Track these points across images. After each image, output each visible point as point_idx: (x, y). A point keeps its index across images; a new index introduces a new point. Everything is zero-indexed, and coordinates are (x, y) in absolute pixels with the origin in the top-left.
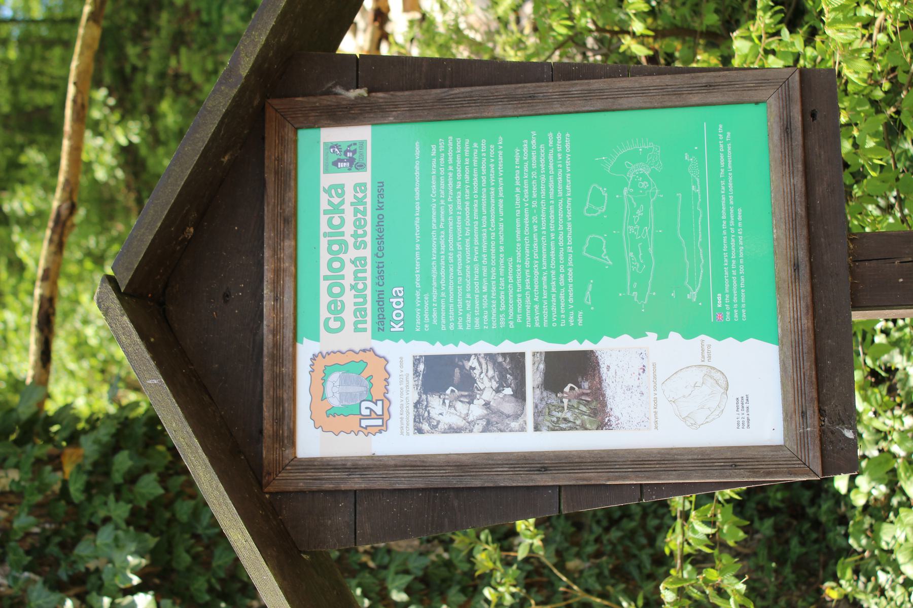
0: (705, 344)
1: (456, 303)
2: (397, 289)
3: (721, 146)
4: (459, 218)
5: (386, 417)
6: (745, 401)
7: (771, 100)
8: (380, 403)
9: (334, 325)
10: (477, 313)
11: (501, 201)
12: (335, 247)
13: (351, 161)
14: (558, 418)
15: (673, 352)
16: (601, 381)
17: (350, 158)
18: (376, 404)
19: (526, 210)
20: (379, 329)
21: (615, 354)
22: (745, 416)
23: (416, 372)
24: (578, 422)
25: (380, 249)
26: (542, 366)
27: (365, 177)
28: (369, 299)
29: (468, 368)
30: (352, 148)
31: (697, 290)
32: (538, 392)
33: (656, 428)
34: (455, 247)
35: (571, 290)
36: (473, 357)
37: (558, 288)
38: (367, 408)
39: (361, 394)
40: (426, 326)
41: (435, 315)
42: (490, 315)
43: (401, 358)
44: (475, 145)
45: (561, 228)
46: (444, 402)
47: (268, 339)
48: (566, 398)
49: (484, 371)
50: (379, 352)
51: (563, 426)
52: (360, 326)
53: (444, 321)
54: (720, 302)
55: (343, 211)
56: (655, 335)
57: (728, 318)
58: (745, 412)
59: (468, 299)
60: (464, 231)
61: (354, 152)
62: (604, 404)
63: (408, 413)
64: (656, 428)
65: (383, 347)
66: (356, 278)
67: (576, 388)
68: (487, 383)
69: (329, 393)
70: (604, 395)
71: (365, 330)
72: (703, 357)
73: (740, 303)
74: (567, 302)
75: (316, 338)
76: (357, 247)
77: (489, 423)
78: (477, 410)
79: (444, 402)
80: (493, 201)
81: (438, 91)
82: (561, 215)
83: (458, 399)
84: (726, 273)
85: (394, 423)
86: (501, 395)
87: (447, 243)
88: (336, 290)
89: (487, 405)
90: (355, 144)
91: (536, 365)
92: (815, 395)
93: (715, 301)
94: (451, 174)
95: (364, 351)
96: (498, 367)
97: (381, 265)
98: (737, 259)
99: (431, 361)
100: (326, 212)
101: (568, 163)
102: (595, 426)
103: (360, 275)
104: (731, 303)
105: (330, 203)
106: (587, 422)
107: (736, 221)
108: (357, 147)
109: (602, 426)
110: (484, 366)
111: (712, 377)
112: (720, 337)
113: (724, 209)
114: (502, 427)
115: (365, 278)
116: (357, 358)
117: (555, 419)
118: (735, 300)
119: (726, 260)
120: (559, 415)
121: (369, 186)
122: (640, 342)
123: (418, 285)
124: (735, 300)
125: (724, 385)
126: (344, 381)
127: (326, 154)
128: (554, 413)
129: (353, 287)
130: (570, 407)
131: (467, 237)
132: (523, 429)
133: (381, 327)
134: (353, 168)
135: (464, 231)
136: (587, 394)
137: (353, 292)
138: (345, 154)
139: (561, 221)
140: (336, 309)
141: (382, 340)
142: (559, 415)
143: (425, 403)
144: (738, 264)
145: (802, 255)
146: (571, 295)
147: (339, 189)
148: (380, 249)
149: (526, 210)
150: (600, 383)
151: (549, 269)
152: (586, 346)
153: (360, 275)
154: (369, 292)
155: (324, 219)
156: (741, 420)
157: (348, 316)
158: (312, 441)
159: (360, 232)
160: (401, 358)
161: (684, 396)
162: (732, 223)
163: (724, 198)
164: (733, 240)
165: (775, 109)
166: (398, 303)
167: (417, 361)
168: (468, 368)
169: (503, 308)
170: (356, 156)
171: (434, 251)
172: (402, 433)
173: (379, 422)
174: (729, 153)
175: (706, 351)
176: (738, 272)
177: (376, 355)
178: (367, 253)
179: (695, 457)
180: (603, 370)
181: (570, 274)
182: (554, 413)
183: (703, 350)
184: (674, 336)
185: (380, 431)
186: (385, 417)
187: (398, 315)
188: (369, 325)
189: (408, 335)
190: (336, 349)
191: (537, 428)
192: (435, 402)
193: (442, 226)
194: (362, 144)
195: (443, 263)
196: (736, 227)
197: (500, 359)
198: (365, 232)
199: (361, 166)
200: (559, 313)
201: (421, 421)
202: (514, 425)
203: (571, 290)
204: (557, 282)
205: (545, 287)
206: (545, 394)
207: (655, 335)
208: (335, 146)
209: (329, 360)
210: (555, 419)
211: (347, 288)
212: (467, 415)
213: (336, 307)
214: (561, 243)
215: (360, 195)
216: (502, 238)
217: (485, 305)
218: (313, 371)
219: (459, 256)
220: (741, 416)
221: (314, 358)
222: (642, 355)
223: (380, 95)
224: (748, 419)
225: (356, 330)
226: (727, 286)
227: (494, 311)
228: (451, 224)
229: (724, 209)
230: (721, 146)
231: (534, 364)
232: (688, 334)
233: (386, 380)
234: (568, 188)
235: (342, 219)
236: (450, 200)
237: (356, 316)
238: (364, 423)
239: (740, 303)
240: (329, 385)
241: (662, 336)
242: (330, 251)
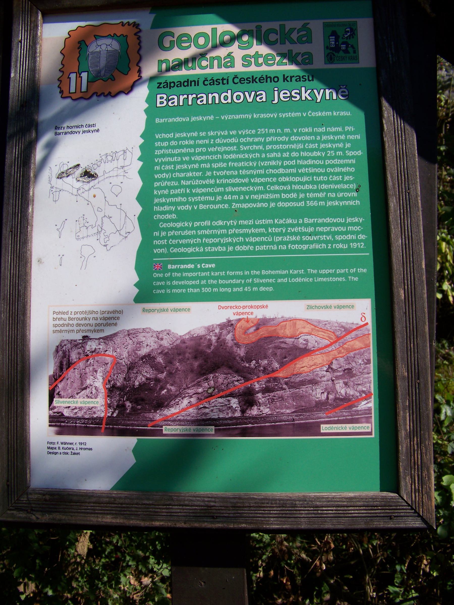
13: (337, 49)
25: (242, 81)
30: (350, 50)
55: (283, 43)
58: (62, 451)
61: (346, 51)
75: (155, 26)
76: (244, 58)
90: (355, 52)
97: (225, 82)
100: (282, 27)
103: (216, 62)
105: (292, 30)
108: (352, 54)
115: (212, 67)
134: (329, 51)
138: (343, 43)
148: (242, 81)
153: (216, 62)
155: (275, 25)
159: (261, 60)
170: (341, 54)
178: (239, 68)
190: (143, 44)
194: (355, 59)
199: (331, 59)
208: (353, 32)
213: (185, 42)
224: (56, 453)
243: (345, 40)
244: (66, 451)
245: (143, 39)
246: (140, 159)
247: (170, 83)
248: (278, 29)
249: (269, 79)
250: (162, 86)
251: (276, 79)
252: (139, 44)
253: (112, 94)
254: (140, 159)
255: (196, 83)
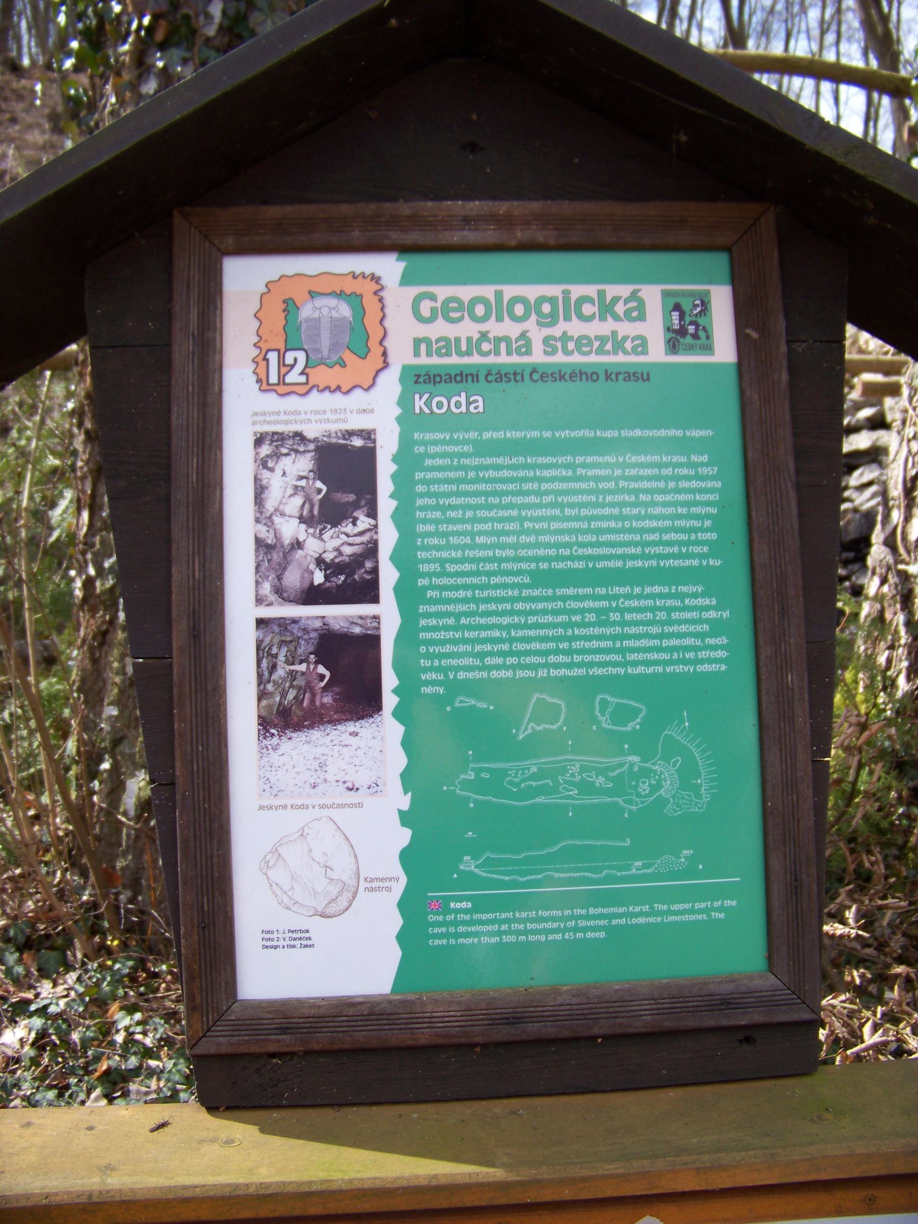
0: (393, 884)
1: (459, 494)
2: (480, 403)
3: (703, 905)
4: (594, 499)
5: (282, 389)
6: (304, 942)
7: (772, 980)
8: (303, 379)
9: (426, 307)
10: (443, 528)
11: (619, 564)
12: (546, 308)
13: (682, 332)
14: (276, 656)
15: (381, 835)
16: (333, 722)
17: (686, 330)
18: (302, 373)
19: (605, 603)
20: (419, 376)
21: (375, 747)
22: (281, 943)
23: (350, 434)
24: (270, 687)
26: (357, 630)
27: (657, 353)
28: (466, 360)
29: (355, 514)
30: (702, 334)
31: (477, 871)
32: (318, 624)
33: (262, 808)
34: (547, 492)
35: (478, 675)
36: (373, 522)
37: (482, 655)
38: (295, 360)
39: (318, 351)
40: (422, 449)
41: (439, 462)
42: (438, 548)
43: (372, 411)
44: (708, 523)
45: (577, 658)
46: (301, 478)
47: (405, 209)
48: (308, 668)
49: (350, 540)
50: (383, 377)
51: (264, 663)
52: (423, 347)
53: (429, 476)
54: (459, 905)
55: (603, 319)
56: (405, 807)
57: (432, 918)
58: (287, 942)
59: (464, 514)
60: (571, 506)
61: (695, 336)
62: (298, 727)
63: (287, 423)
64: (262, 808)
65: (390, 384)
66: (498, 340)
67: (323, 684)
68: (332, 544)
69: (319, 302)
70: (311, 727)
71: (417, 354)
72: (372, 880)
73: (458, 935)
74: (457, 669)
75: (406, 280)
76: (546, 341)
77: (269, 548)
78: (290, 529)
79: (301, 478)
80: (620, 551)
81: (791, 466)
82: (597, 658)
83: (308, 499)
84: (504, 916)
85: (271, 401)
86: (312, 567)
87: (552, 479)
88: (480, 310)
89: (298, 545)
90: (708, 337)
91: (360, 621)
92: (315, 1047)
93: (460, 899)
94: (662, 485)
95: (385, 354)
96: (357, 561)
97: (519, 377)
98: (526, 932)
99: (367, 457)
100: (601, 294)
101: (679, 669)
102: (264, 714)
103: (503, 346)
104: (456, 923)
105: (615, 300)
106: (271, 701)
107: (585, 930)
108: (704, 340)
109: (265, 724)
110: (358, 540)
111: (340, 893)
112: (403, 905)
113: (605, 911)
114: (262, 569)
115: (497, 353)
116: (373, 343)
117: (275, 650)
118: (461, 929)
119: (524, 915)
120: (281, 658)
121: (642, 359)
122: (395, 784)
123: (487, 435)
124: (461, 929)
125: (329, 911)
126: (337, 325)
127: (691, 294)
128: (284, 650)
129: (484, 336)
130: (293, 675)
131: (562, 511)
132: (259, 601)
133: (421, 379)
134: (671, 335)
135: (571, 506)
136: (313, 701)
137: (476, 336)
138: (691, 323)
139: (588, 658)
140: (449, 311)
141: (402, 380)
142: (281, 658)
143: (301, 449)
144: (518, 933)
145: (532, 1029)
146: (470, 675)
147: (638, 313)
149: (605, 603)
150: (330, 722)
151: (511, 640)
152: (389, 700)
153: (503, 346)
154: (476, 359)
155: (591, 290)
156: (275, 936)
157: (439, 329)
158: (247, 279)
159: (571, 346)
160: (372, 411)
161: (310, 851)
162: (582, 923)
163: (621, 910)
164: (555, 925)
165: (758, 983)
166: (458, 405)
167: (368, 435)
168: (355, 514)
169: (451, 568)
170: (689, 340)
171: (540, 460)
172: (255, 414)
173: (274, 379)
174: (692, 917)
175: (381, 884)
176: (505, 933)
177: (378, 372)
178: (538, 356)
179: (215, 869)
180: (351, 726)
181: (503, 674)
182: (284, 650)
183: (382, 880)
184: (404, 836)
185: (259, 381)
186: (282, 388)
187: (440, 405)
188: (424, 360)
189: (408, 420)
190: (387, 311)
191: (261, 623)
192: (304, 464)
193: (580, 471)
194: (708, 348)
195: (521, 474)
196: (576, 929)
197: (369, 565)
198: (571, 353)
199: (674, 346)
200: (441, 656)
201: (274, 443)
202: (266, 588)
203: (478, 675)
204: (491, 654)
205: (484, 634)
206: (314, 635)
207: (405, 807)
208: (705, 307)
209: (370, 303)
210: (275, 650)
211: (483, 327)
212: (283, 514)
213: (454, 310)
214: (552, 659)
215: (628, 345)
216: (561, 565)
217: (454, 540)
218: (355, 277)
219: (533, 499)
220: (281, 936)
221: (375, 279)
222: (375, 787)
223: (785, 377)
224: (276, 947)
225: (417, 342)
226: (484, 917)
227: (445, 554)
228: (584, 486)
229: (605, 911)
230: (703, 905)
231: (361, 618)
232: (407, 857)
233: (339, 388)
234: (640, 669)
235: (590, 318)
236: (622, 484)
237: (437, 341)
238: (273, 357)
239: (458, 935)
240: (332, 302)
241: (405, 818)
242: (541, 300)
243: (693, 318)
244: (292, 943)
245: (388, 301)
246: (392, 496)
247: (434, 376)
248: (595, 297)
249: (584, 377)
250: (421, 380)
251: (595, 377)
252: (382, 309)
253: (344, 389)
254: (392, 496)
255: (475, 378)
